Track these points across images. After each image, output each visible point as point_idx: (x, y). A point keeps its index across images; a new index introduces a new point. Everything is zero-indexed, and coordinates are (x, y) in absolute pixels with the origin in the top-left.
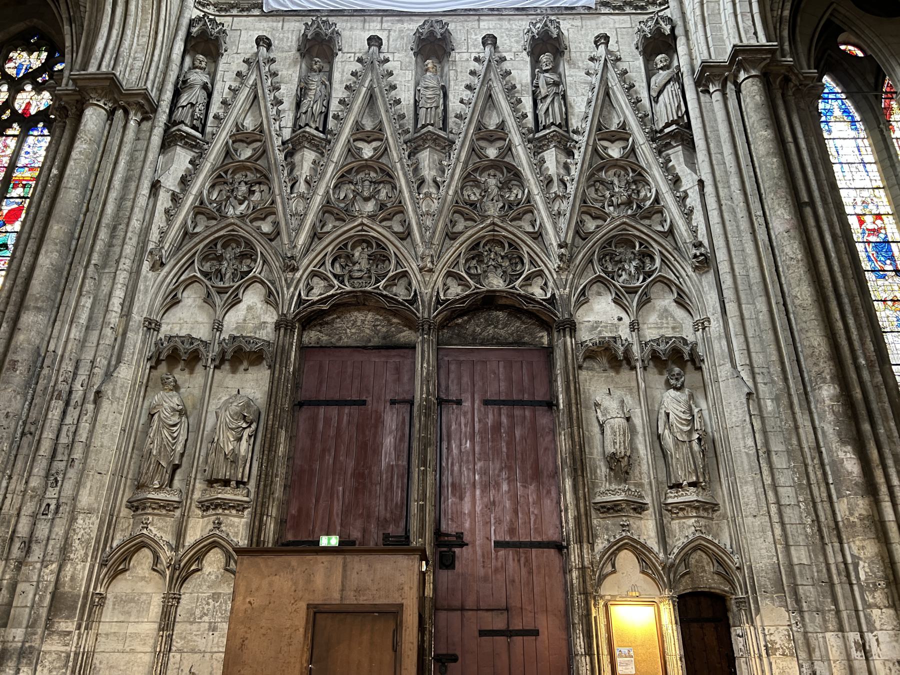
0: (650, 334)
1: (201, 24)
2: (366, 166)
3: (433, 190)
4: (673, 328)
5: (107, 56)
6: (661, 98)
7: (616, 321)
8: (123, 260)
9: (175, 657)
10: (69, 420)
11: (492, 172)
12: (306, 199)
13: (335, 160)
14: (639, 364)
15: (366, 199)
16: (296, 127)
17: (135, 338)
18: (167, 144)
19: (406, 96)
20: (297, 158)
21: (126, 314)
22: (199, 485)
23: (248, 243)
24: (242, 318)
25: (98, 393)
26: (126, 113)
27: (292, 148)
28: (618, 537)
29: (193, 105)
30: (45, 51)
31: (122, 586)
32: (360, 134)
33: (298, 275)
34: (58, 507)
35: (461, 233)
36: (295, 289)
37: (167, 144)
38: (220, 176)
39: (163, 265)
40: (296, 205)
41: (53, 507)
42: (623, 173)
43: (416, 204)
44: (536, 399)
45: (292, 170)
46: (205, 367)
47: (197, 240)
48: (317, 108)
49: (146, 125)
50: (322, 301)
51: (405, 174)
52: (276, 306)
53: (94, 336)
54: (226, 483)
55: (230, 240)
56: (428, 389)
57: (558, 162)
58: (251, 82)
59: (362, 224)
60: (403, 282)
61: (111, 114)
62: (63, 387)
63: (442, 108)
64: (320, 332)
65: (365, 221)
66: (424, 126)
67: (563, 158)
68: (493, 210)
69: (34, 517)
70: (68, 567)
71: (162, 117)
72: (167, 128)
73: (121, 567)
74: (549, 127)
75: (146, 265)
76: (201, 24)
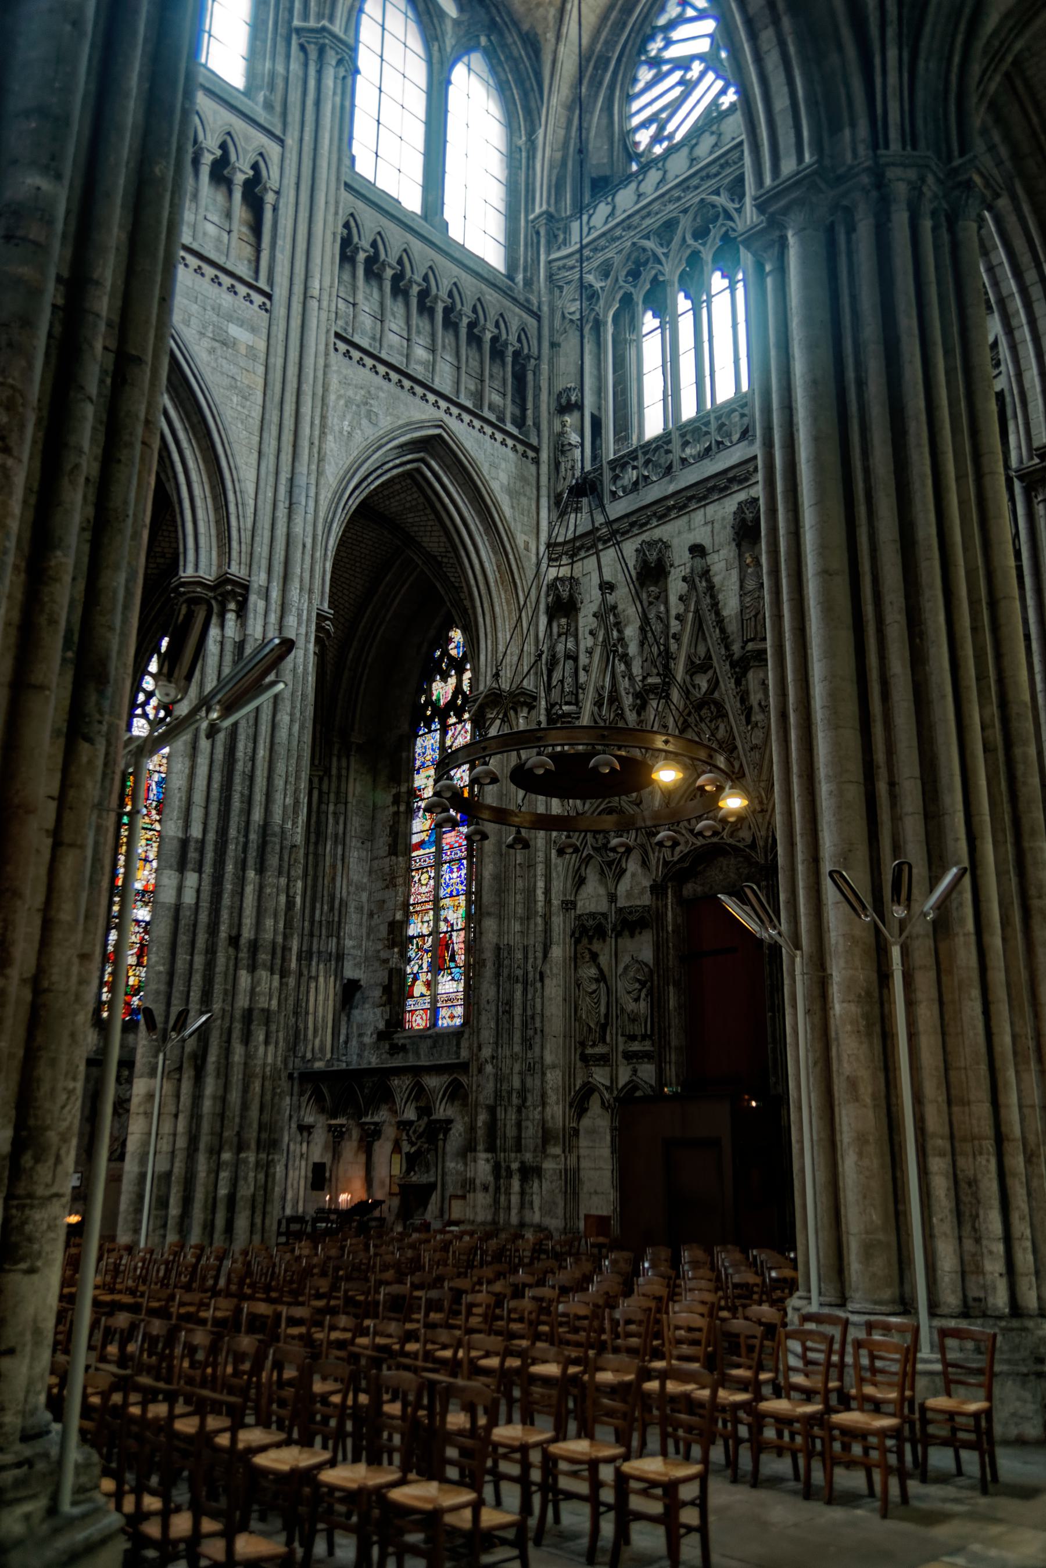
21: (548, 901)
25: (541, 974)
31: (586, 1122)
75: (554, 852)
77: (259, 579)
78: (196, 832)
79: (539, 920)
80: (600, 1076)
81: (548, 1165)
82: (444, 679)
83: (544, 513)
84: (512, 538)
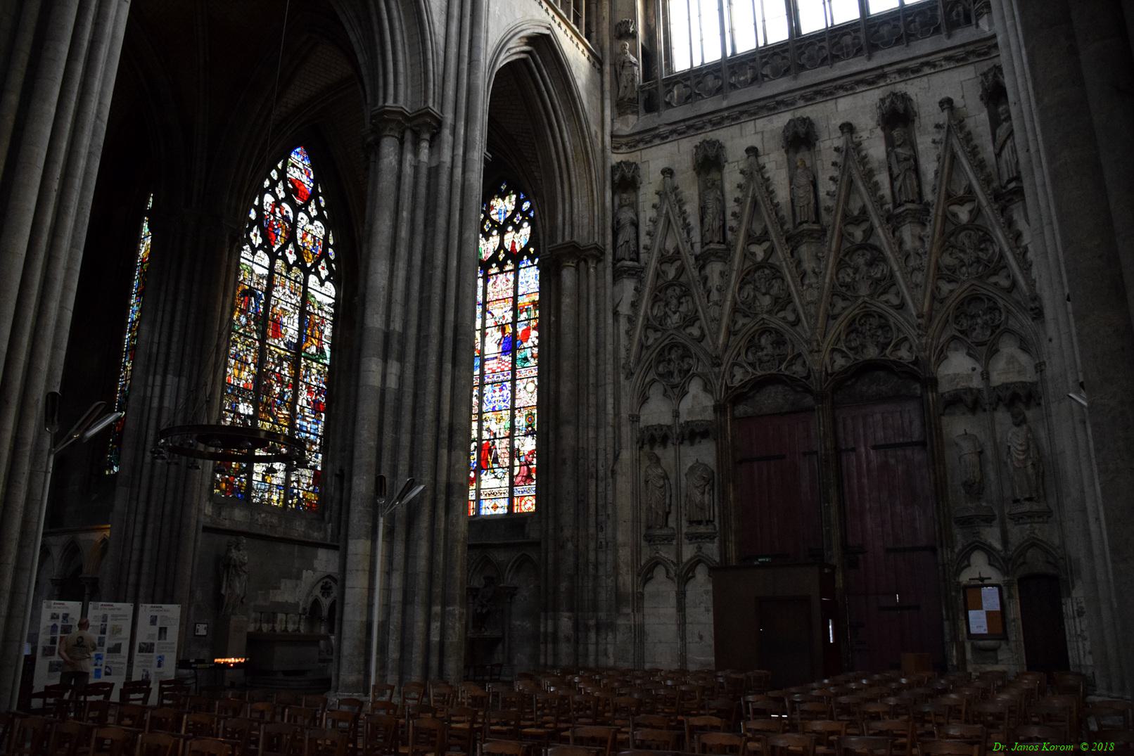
0: (997, 379)
1: (620, 170)
2: (760, 266)
3: (813, 280)
4: (1019, 372)
5: (567, 227)
6: (1003, 154)
7: (970, 372)
8: (607, 376)
9: (689, 627)
10: (600, 490)
11: (860, 252)
12: (719, 304)
13: (735, 268)
14: (987, 407)
15: (764, 294)
16: (704, 244)
17: (626, 431)
18: (618, 275)
19: (782, 194)
20: (708, 270)
21: (617, 414)
22: (684, 523)
23: (684, 347)
24: (690, 405)
25: (613, 472)
26: (586, 262)
27: (702, 261)
28: (970, 542)
29: (627, 242)
30: (513, 194)
31: (649, 588)
32: (751, 239)
33: (723, 368)
34: (607, 543)
35: (840, 314)
36: (723, 379)
37: (618, 275)
38: (656, 295)
39: (632, 374)
40: (714, 312)
41: (604, 543)
42: (973, 233)
43: (801, 296)
44: (914, 440)
45: (705, 284)
46: (673, 444)
47: (653, 349)
48: (717, 224)
49: (601, 266)
50: (743, 386)
51: (790, 272)
52: (712, 393)
53: (602, 434)
54: (700, 523)
55: (672, 346)
56: (825, 446)
57: (913, 235)
58: (664, 212)
59: (763, 319)
60: (800, 361)
61: (577, 268)
62: (594, 470)
63: (813, 202)
64: (746, 405)
65: (765, 316)
66: (801, 223)
67: (918, 230)
68: (864, 290)
69: (596, 550)
70: (620, 578)
71: (610, 258)
72: (614, 265)
73: (649, 576)
74: (903, 205)
75: (622, 377)
76: (620, 170)
77: (449, 117)
78: (397, 326)
79: (610, 429)
80: (667, 553)
81: (621, 621)
82: (487, 236)
83: (608, 112)
84: (588, 127)
